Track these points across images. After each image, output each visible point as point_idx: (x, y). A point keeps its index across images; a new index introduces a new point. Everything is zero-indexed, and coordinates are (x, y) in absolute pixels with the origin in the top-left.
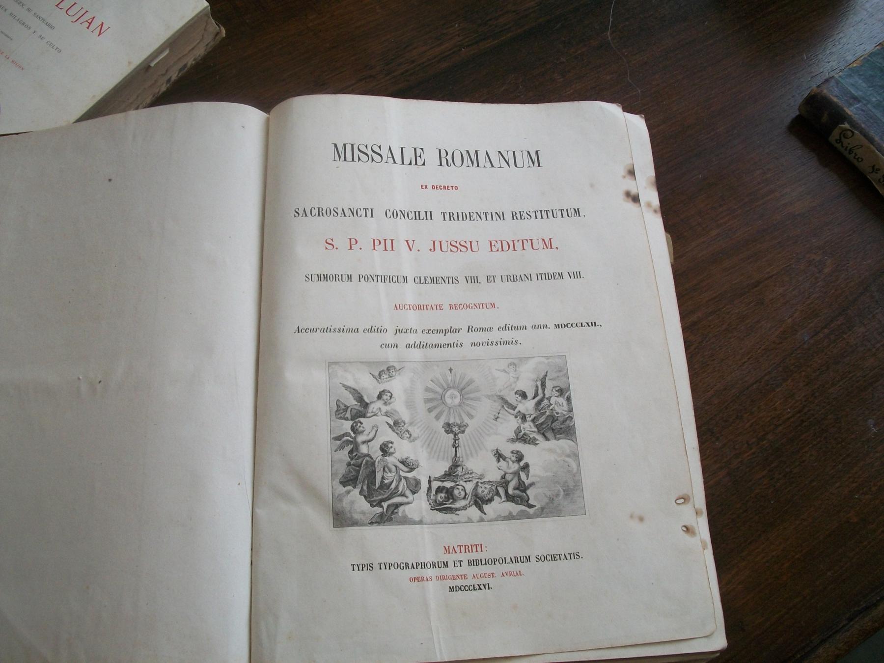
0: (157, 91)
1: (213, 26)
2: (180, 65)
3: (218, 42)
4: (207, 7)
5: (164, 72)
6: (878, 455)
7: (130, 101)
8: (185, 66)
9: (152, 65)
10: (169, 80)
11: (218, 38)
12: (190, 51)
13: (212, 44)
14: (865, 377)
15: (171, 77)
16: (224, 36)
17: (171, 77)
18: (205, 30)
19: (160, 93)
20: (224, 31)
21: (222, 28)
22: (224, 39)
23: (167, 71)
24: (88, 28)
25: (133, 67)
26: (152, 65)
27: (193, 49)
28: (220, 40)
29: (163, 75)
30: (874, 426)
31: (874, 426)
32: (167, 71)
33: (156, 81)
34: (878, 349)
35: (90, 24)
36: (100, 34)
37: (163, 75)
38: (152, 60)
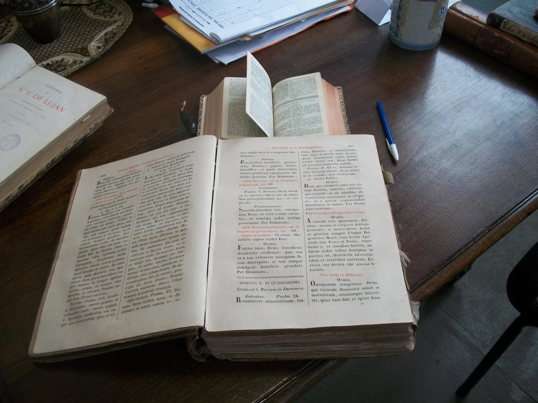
0: (86, 132)
1: (108, 108)
2: (95, 123)
3: (111, 114)
4: (106, 99)
5: (88, 125)
6: (404, 237)
7: (75, 136)
8: (97, 123)
9: (84, 121)
10: (90, 129)
11: (111, 113)
12: (99, 117)
13: (109, 114)
14: (395, 209)
15: (91, 127)
16: (113, 112)
17: (91, 127)
18: (105, 109)
19: (87, 133)
20: (113, 110)
21: (112, 108)
22: (113, 113)
23: (90, 125)
24: (57, 109)
25: (76, 121)
26: (84, 121)
27: (100, 116)
28: (111, 113)
29: (88, 126)
30: (402, 226)
31: (402, 226)
32: (90, 125)
33: (85, 129)
34: (401, 199)
35: (57, 108)
36: (62, 111)
37: (88, 126)
38: (84, 119)
